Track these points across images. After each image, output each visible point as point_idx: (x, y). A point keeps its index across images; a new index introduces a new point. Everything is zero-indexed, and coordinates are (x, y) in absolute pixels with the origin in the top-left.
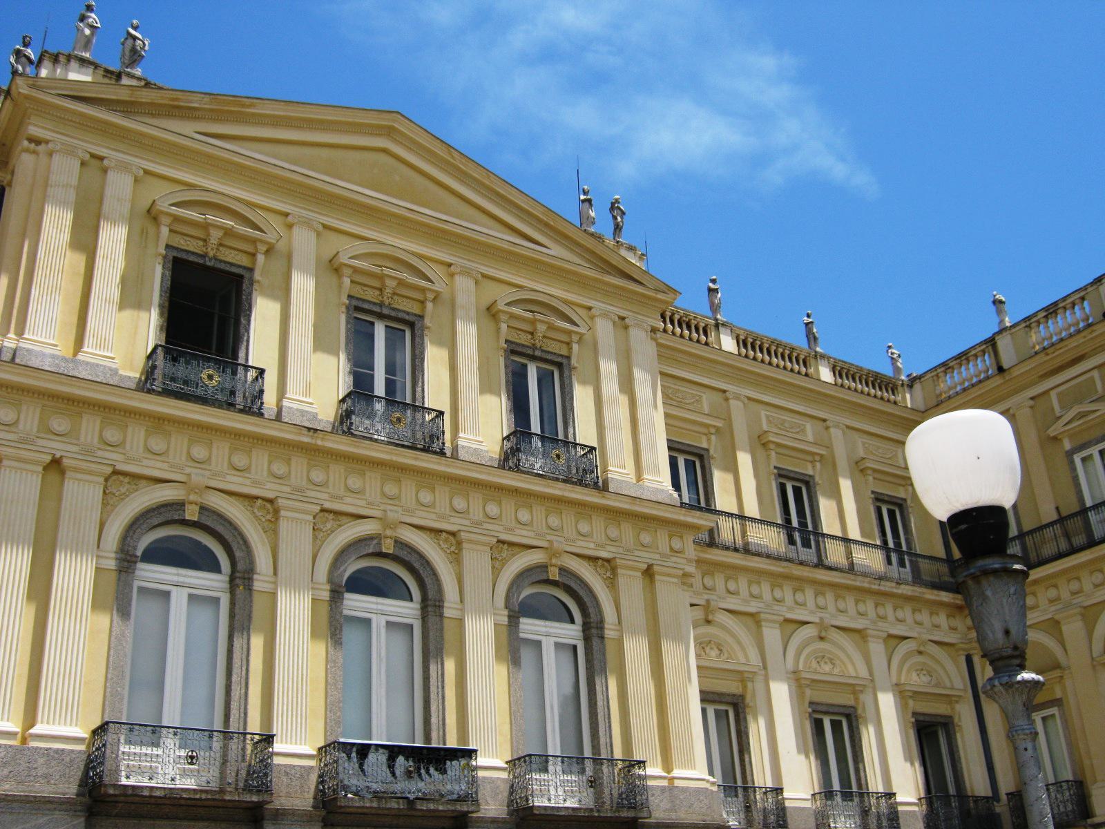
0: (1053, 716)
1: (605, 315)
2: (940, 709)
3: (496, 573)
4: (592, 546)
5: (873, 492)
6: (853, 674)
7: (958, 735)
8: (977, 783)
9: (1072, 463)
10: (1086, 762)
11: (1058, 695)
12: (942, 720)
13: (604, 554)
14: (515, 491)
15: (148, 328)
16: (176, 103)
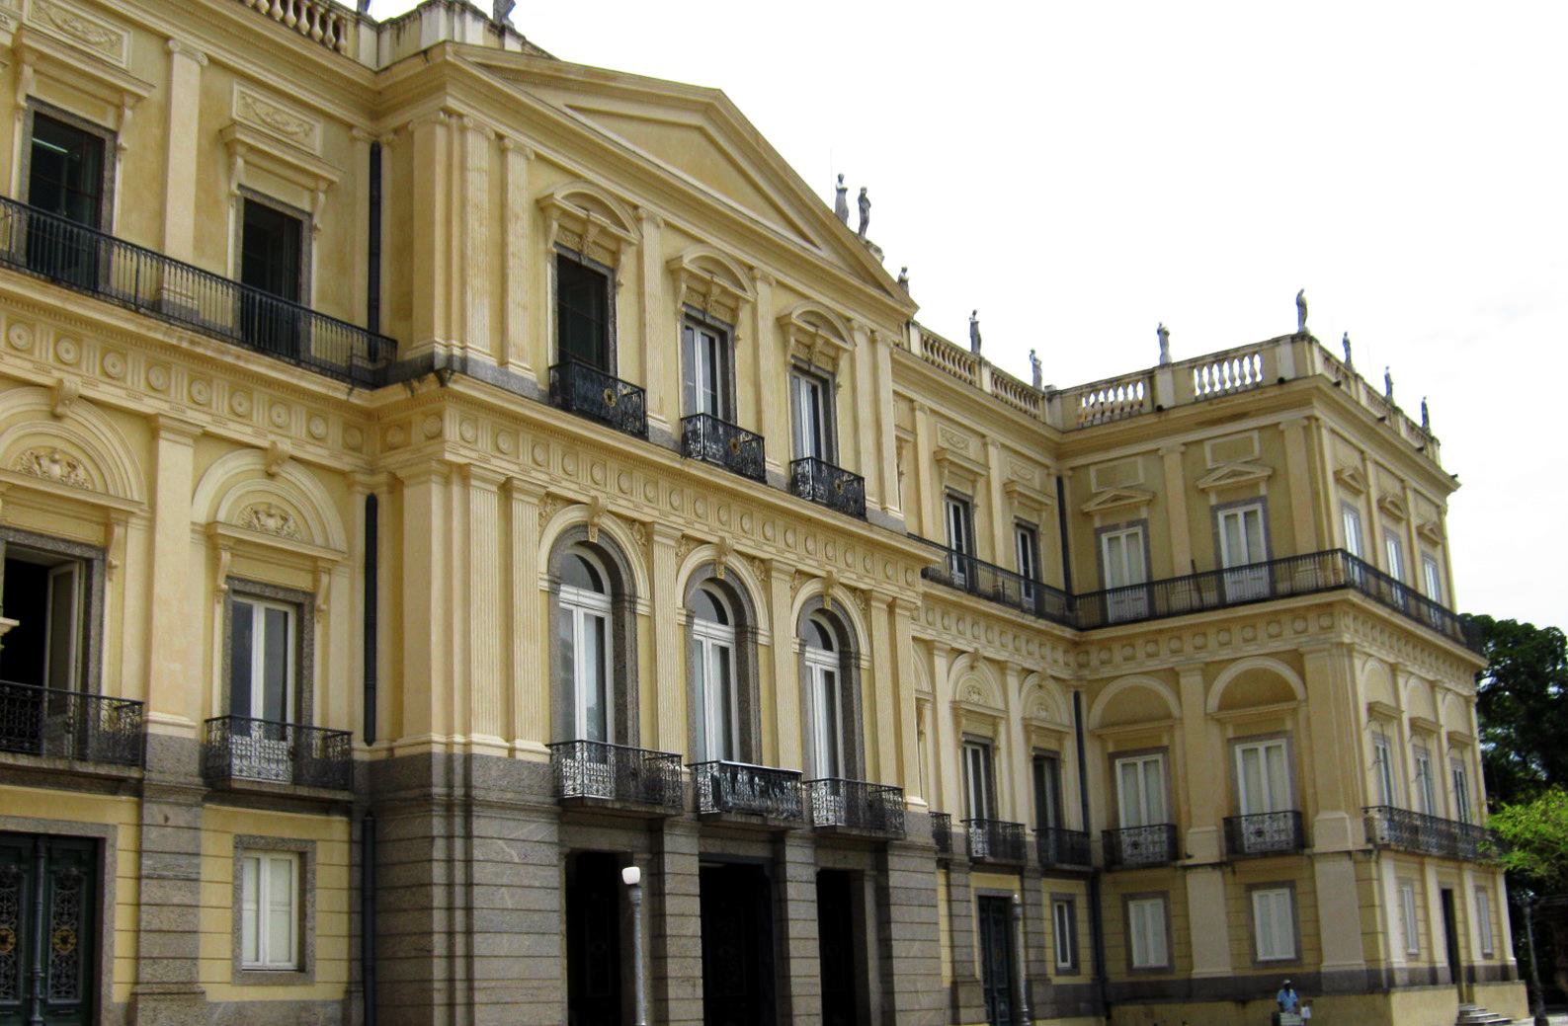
0: (1157, 761)
2: (1051, 745)
4: (855, 577)
5: (1016, 517)
6: (1059, 721)
7: (1063, 772)
8: (1073, 820)
9: (1215, 519)
10: (1184, 809)
11: (1165, 741)
12: (1051, 755)
13: (862, 586)
16: (557, 74)
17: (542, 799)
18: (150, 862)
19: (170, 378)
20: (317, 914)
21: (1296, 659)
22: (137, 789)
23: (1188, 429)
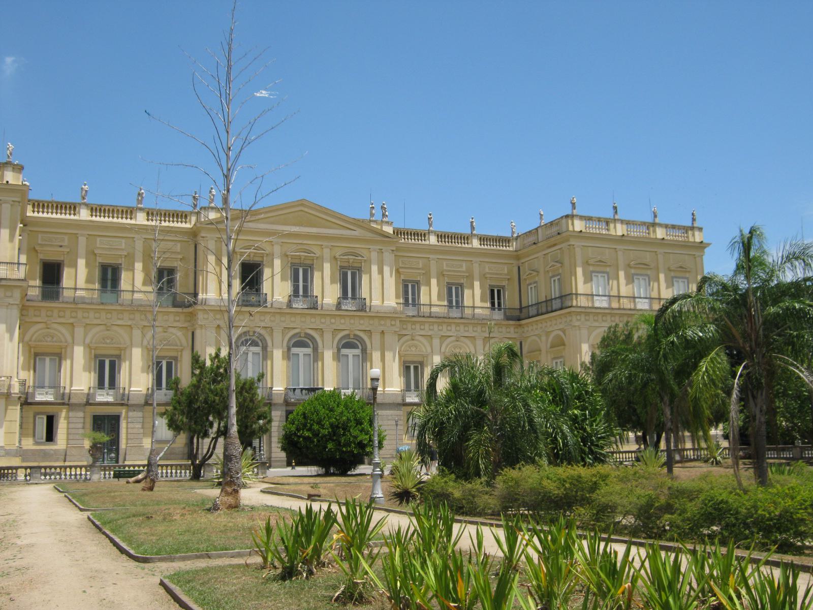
1: (375, 250)
3: (333, 338)
14: (340, 315)
15: (237, 284)
17: (260, 395)
21: (564, 331)
23: (543, 250)
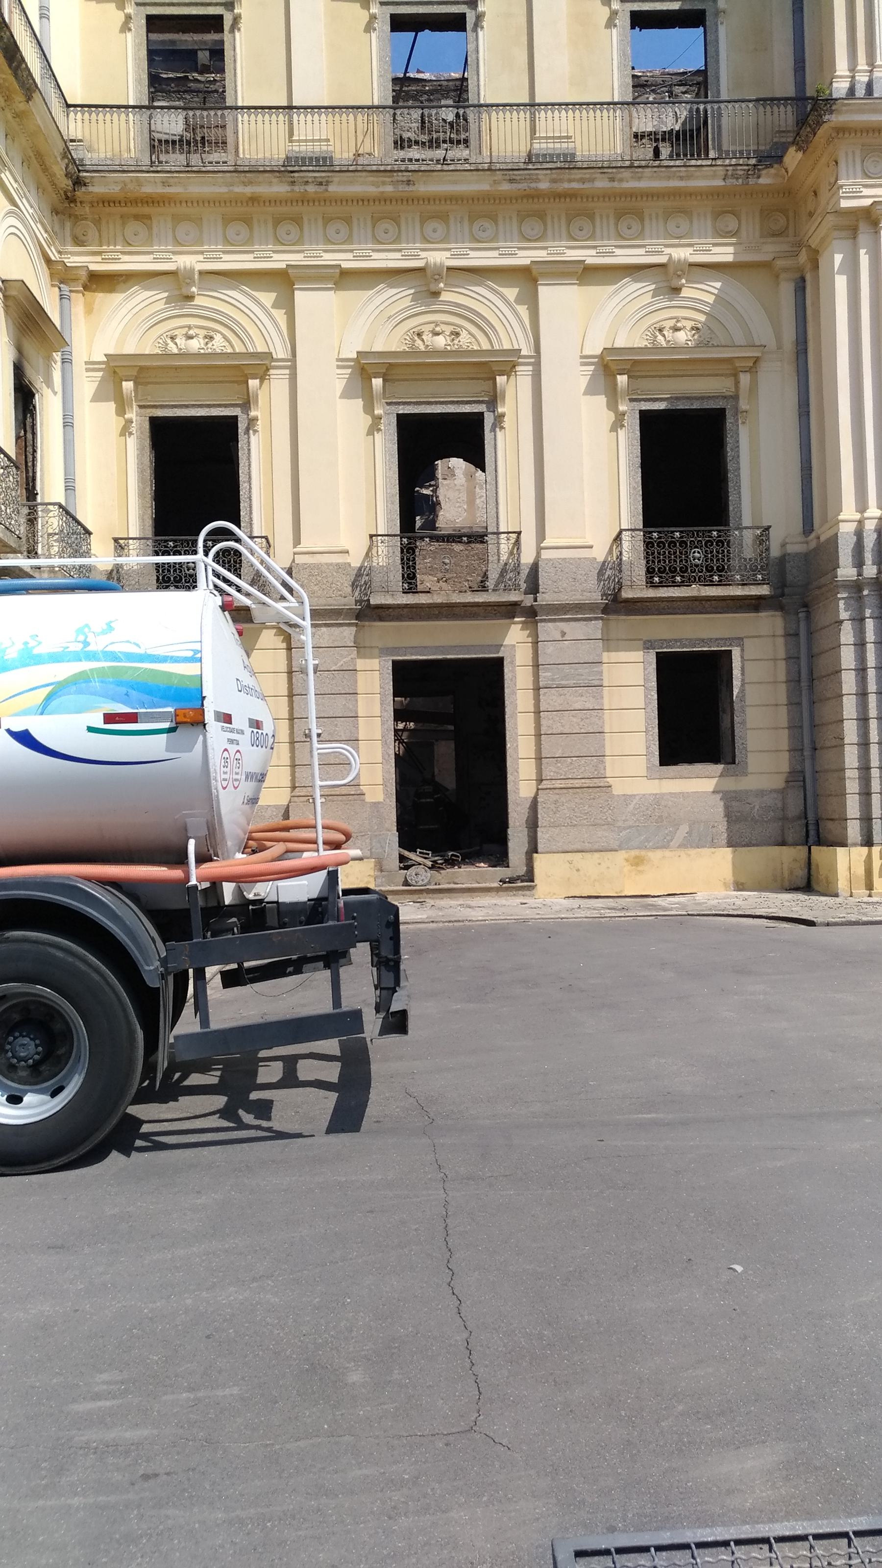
18: (549, 674)
19: (594, 227)
20: (748, 710)
22: (532, 614)
